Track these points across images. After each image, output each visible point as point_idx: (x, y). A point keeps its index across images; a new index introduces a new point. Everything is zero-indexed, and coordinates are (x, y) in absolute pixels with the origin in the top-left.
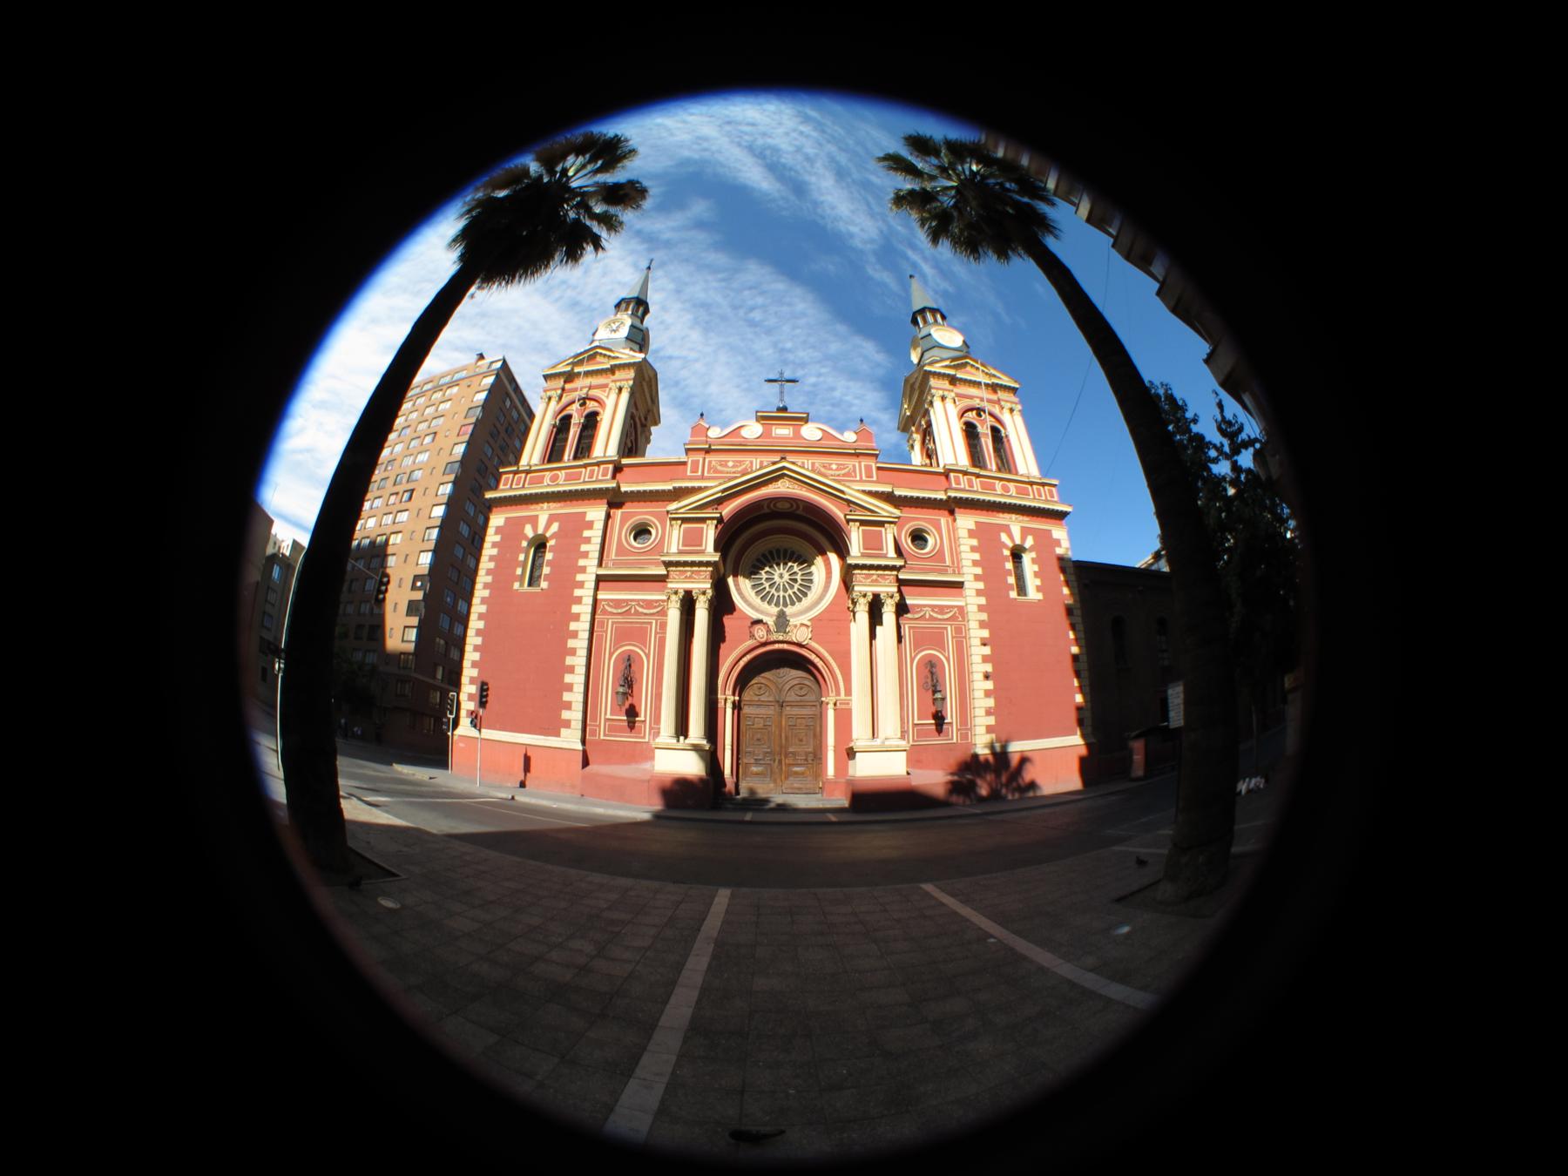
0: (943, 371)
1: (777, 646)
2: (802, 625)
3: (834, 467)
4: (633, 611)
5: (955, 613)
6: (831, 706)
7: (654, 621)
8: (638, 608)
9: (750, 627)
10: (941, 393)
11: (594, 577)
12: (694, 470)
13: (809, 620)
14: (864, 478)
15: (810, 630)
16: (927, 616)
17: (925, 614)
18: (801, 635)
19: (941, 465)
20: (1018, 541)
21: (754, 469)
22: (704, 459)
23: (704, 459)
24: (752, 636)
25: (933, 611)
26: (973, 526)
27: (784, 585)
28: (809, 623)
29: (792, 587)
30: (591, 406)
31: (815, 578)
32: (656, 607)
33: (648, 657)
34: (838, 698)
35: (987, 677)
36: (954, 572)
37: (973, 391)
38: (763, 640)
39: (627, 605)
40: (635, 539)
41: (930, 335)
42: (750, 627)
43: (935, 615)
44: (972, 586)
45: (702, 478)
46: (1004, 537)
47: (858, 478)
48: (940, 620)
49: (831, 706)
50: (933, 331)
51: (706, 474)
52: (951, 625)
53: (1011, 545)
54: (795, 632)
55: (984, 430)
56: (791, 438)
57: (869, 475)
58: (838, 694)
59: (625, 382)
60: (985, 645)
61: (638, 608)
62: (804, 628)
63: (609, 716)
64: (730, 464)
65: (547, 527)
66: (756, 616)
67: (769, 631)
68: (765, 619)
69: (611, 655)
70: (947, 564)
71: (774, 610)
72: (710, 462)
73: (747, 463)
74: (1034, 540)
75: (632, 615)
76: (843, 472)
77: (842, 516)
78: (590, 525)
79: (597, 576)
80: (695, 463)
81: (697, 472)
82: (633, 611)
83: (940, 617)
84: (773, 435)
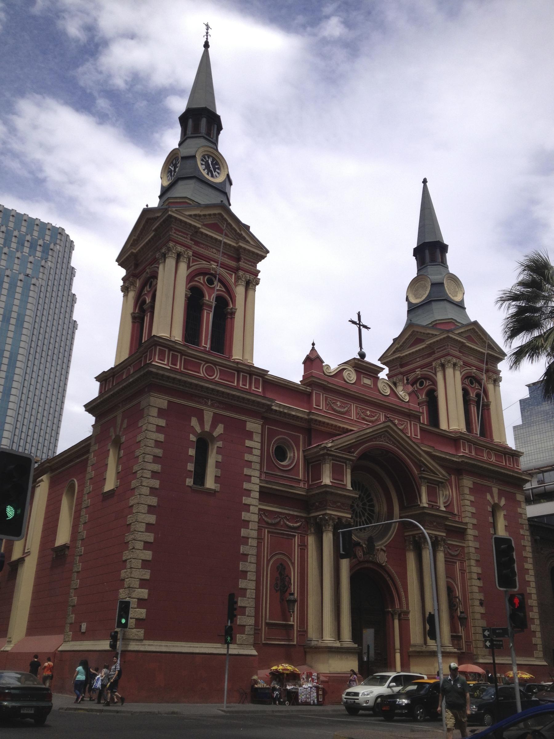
1: (366, 565)
2: (382, 549)
8: (285, 521)
10: (454, 360)
11: (257, 488)
13: (385, 546)
18: (382, 558)
20: (496, 501)
25: (449, 548)
26: (472, 486)
27: (359, 512)
29: (364, 515)
30: (218, 288)
31: (377, 509)
32: (296, 522)
35: (481, 604)
37: (472, 360)
39: (277, 518)
44: (471, 532)
46: (489, 497)
53: (492, 503)
54: (378, 554)
55: (473, 395)
60: (479, 579)
61: (285, 521)
62: (382, 553)
63: (268, 621)
65: (214, 426)
69: (268, 561)
74: (506, 500)
78: (250, 435)
79: (260, 486)
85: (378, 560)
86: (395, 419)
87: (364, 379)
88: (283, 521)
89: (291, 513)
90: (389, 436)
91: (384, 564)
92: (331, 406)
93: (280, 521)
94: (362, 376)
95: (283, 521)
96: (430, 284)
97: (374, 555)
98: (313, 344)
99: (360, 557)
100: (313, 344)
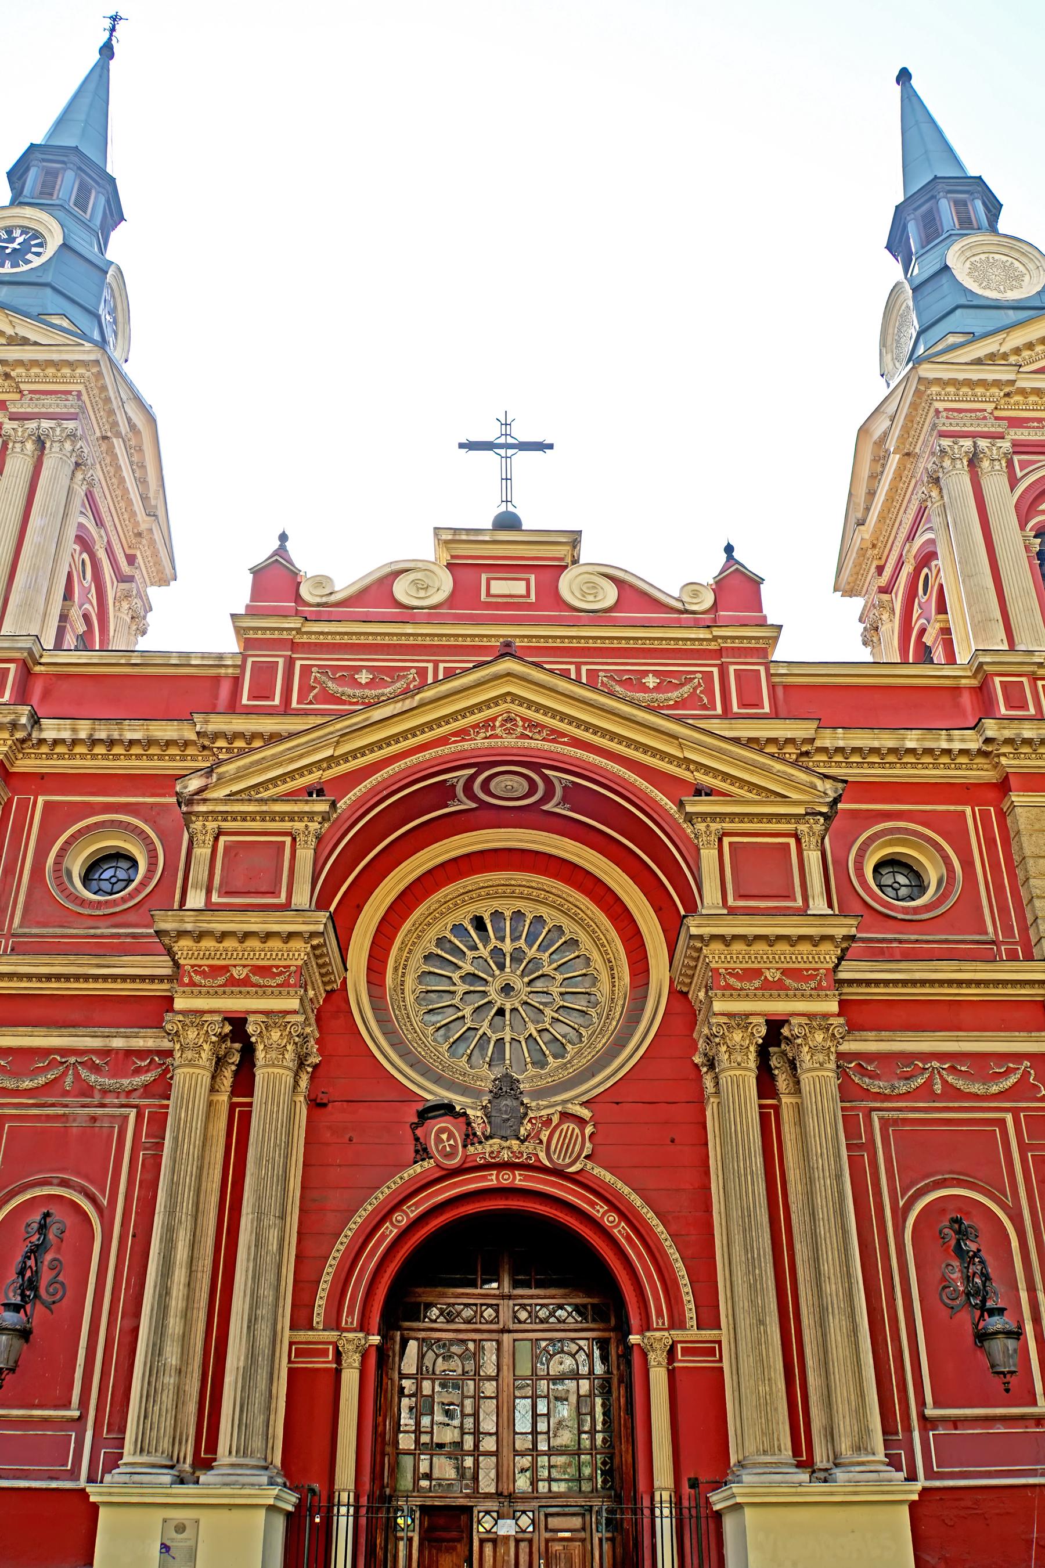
0: (975, 374)
2: (565, 1116)
3: (651, 681)
4: (69, 1079)
5: (1026, 1074)
6: (657, 1362)
7: (133, 1113)
8: (84, 1073)
9: (414, 1126)
12: (263, 691)
14: (735, 709)
15: (589, 1130)
16: (938, 1088)
17: (930, 1078)
19: (962, 657)
21: (430, 680)
22: (290, 663)
23: (290, 663)
24: (422, 1152)
25: (953, 1069)
28: (586, 1114)
32: (138, 1071)
33: (106, 1215)
34: (677, 1334)
36: (1013, 957)
38: (455, 1162)
40: (86, 880)
41: (946, 268)
42: (414, 1126)
43: (960, 1084)
45: (286, 710)
47: (719, 711)
48: (975, 1097)
49: (657, 1362)
50: (955, 257)
51: (294, 704)
52: (1015, 1111)
54: (544, 1136)
56: (529, 606)
57: (750, 701)
58: (677, 1322)
59: (52, 423)
61: (84, 1073)
62: (570, 1126)
64: (364, 677)
66: (434, 1094)
67: (470, 1137)
68: (458, 1100)
70: (991, 936)
71: (486, 1076)
72: (306, 670)
73: (413, 671)
75: (66, 1093)
76: (675, 695)
77: (672, 807)
80: (264, 674)
81: (270, 697)
82: (69, 1079)
83: (977, 1088)
84: (483, 597)
85: (542, 1156)
86: (646, 673)
87: (493, 582)
88: (77, 1075)
89: (118, 1043)
90: (530, 714)
91: (570, 1170)
92: (324, 690)
93: (65, 1074)
94: (484, 577)
95: (77, 1075)
96: (911, 292)
97: (522, 1142)
98: (283, 537)
99: (449, 1156)
100: (283, 537)
